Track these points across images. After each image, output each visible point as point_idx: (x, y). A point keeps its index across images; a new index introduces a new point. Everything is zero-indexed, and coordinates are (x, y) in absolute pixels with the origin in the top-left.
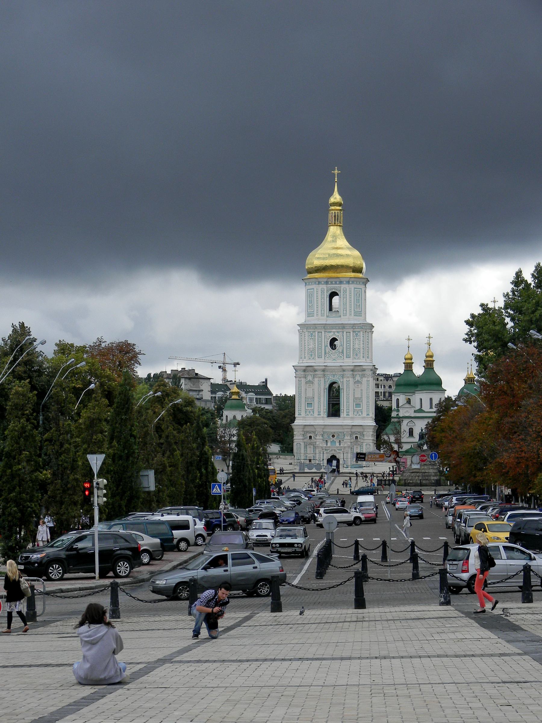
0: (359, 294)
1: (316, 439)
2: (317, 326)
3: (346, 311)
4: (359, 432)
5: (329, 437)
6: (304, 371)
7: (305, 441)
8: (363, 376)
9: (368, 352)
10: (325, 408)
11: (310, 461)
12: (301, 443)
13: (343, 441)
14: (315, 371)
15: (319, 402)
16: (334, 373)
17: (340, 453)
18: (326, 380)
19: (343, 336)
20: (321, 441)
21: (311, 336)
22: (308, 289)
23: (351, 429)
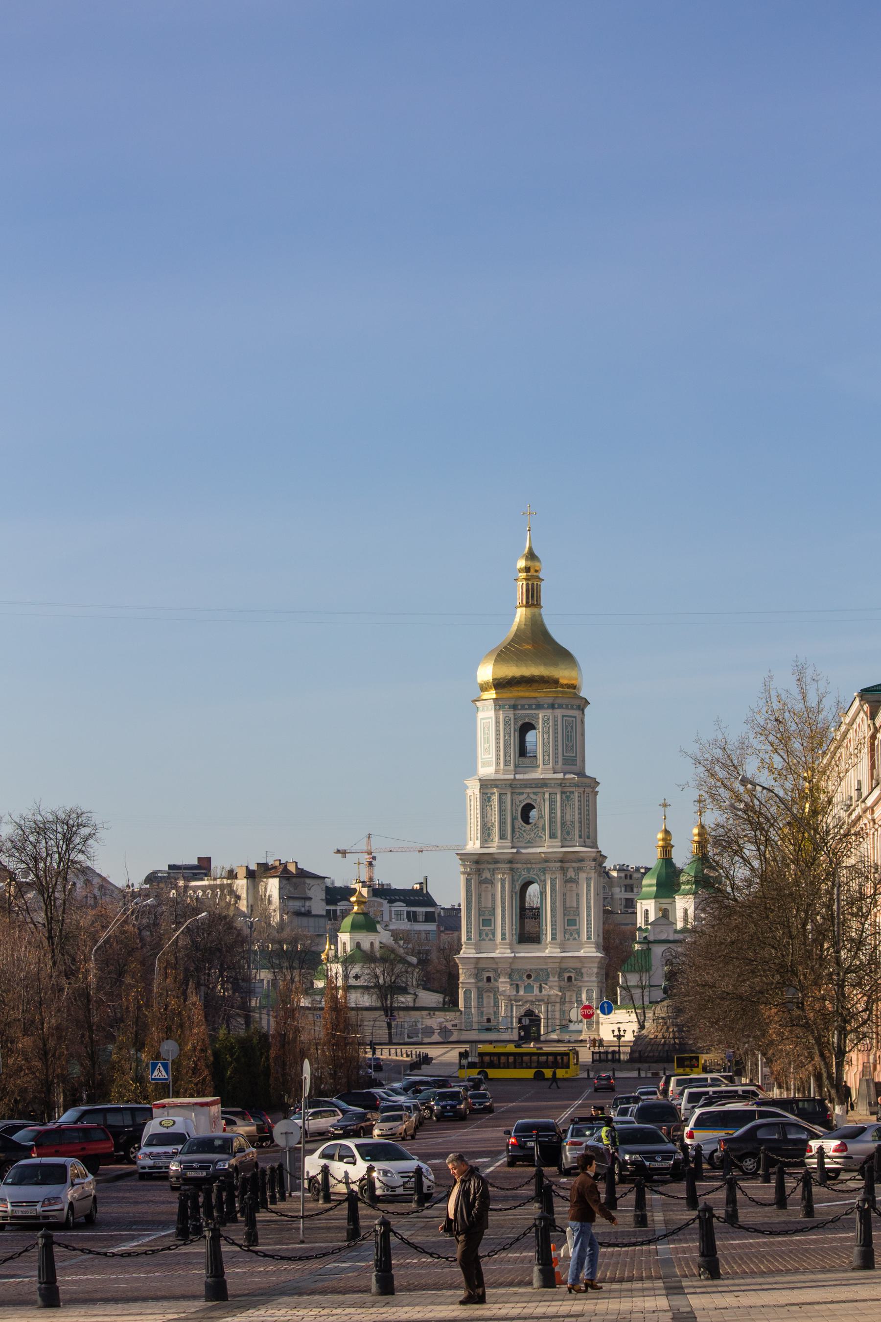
0: (572, 727)
2: (498, 783)
3: (549, 756)
5: (521, 979)
6: (477, 862)
8: (580, 869)
9: (589, 828)
10: (514, 927)
11: (489, 1020)
14: (497, 862)
16: (529, 866)
18: (516, 878)
23: (560, 963)
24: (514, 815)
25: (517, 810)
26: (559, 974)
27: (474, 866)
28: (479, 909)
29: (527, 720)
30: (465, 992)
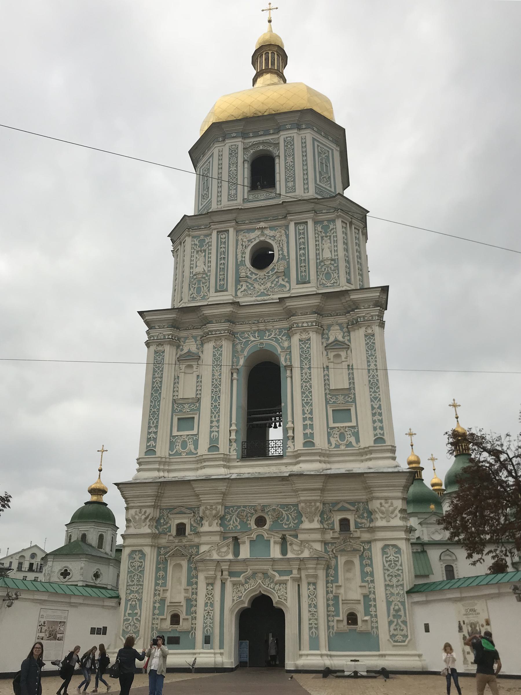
0: (328, 157)
1: (198, 534)
3: (294, 181)
4: (353, 503)
5: (244, 524)
7: (163, 541)
9: (361, 275)
10: (234, 427)
11: (175, 619)
12: (147, 550)
13: (296, 536)
14: (206, 321)
15: (215, 409)
16: (262, 327)
17: (285, 583)
18: (239, 347)
19: (287, 236)
20: (216, 539)
21: (201, 246)
22: (200, 168)
24: (240, 259)
25: (244, 253)
26: (322, 514)
27: (167, 332)
28: (174, 401)
29: (261, 148)
30: (130, 555)
